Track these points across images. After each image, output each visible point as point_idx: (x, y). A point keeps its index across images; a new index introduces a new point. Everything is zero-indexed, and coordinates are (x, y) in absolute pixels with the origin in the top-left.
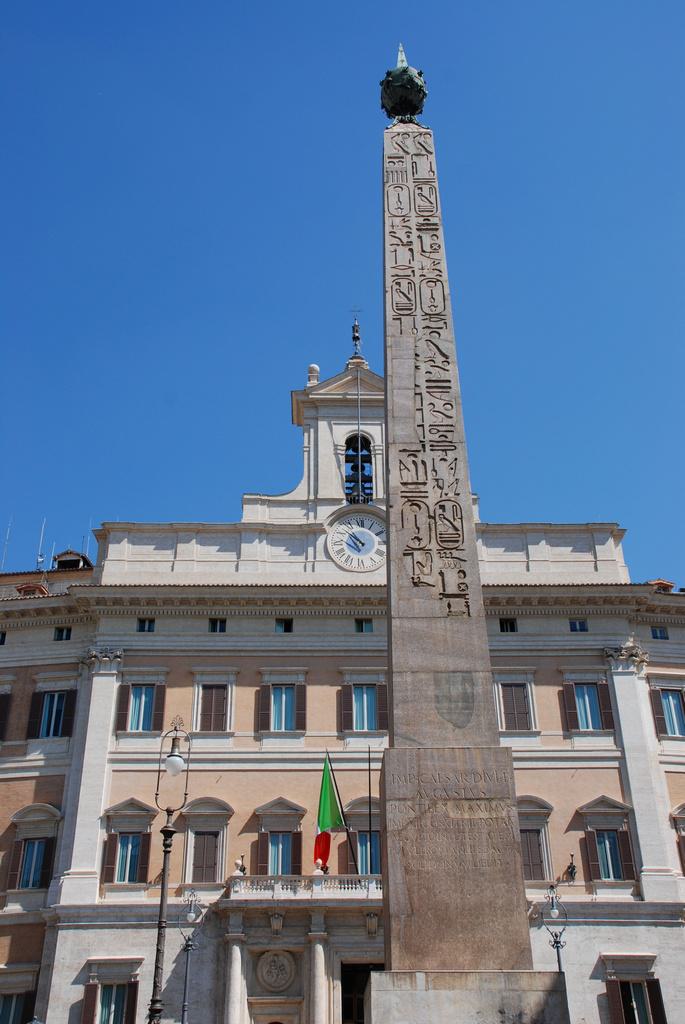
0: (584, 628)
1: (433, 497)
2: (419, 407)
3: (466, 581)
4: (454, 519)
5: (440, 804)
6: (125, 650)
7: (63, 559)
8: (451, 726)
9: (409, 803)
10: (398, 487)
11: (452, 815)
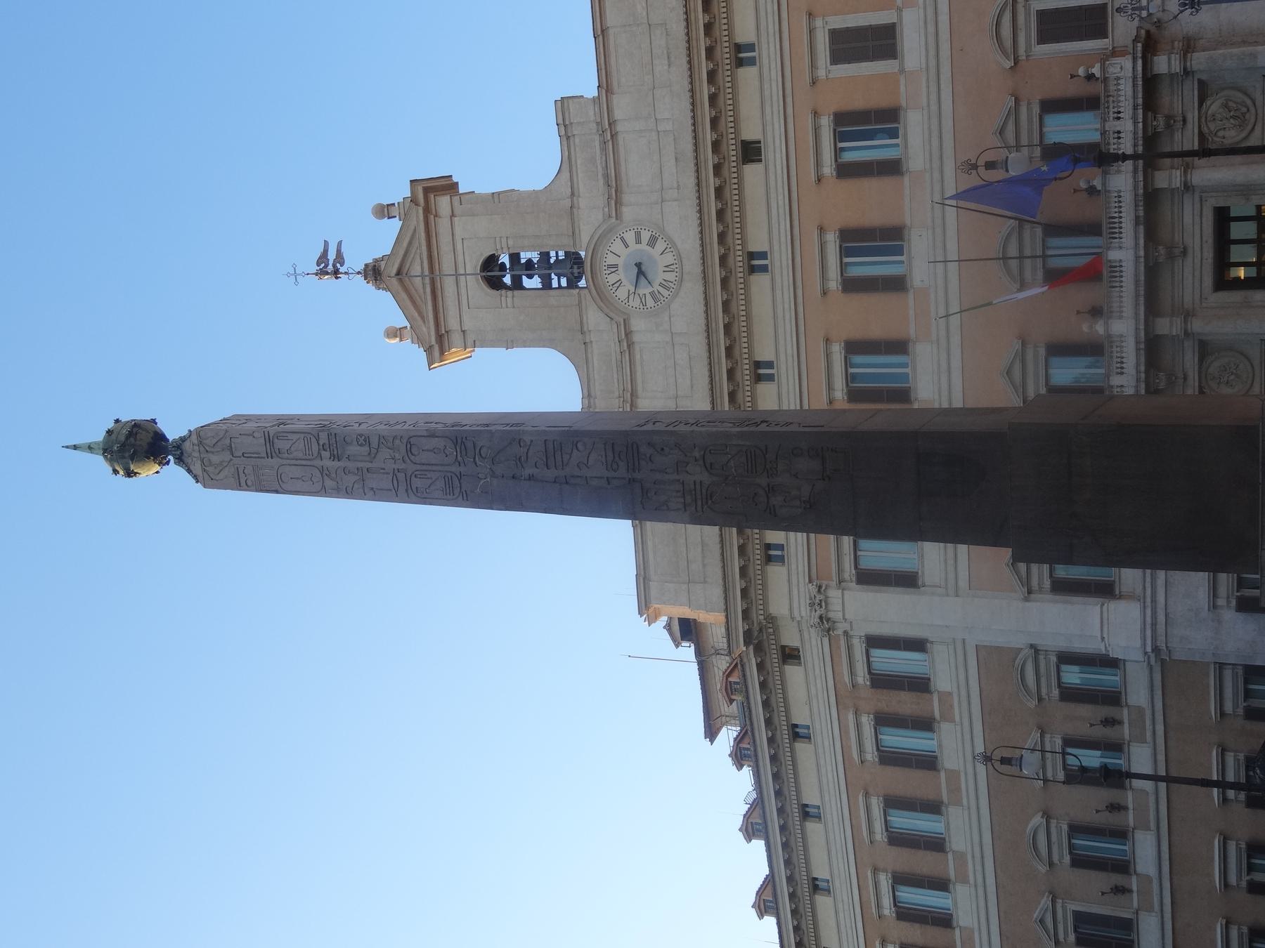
4: (727, 453)
6: (810, 581)
7: (678, 634)
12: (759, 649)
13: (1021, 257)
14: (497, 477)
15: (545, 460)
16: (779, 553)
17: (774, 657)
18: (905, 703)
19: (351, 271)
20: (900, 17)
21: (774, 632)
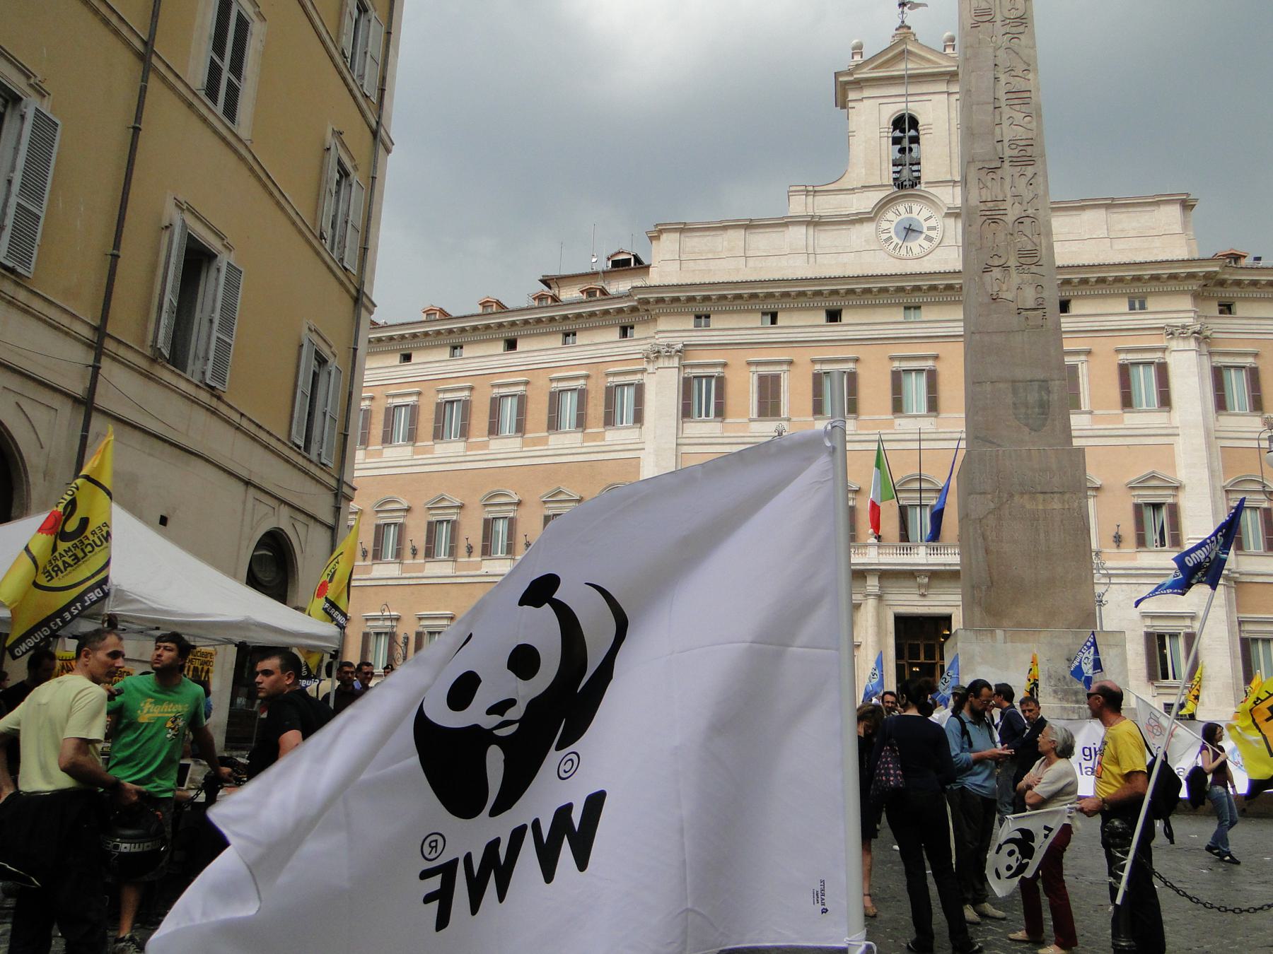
0: (1143, 307)
1: (1013, 212)
2: (997, 121)
3: (1043, 295)
4: (1033, 235)
5: (1017, 498)
6: (685, 345)
8: (1027, 430)
9: (989, 496)
10: (977, 206)
11: (1028, 506)
12: (634, 309)
13: (921, 490)
14: (994, 52)
15: (1014, 90)
16: (703, 324)
17: (626, 321)
18: (596, 408)
19: (905, 16)
20: (1085, 413)
21: (645, 320)
